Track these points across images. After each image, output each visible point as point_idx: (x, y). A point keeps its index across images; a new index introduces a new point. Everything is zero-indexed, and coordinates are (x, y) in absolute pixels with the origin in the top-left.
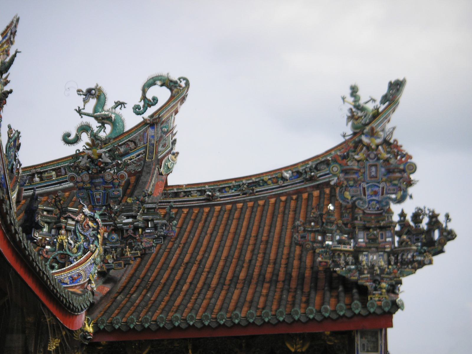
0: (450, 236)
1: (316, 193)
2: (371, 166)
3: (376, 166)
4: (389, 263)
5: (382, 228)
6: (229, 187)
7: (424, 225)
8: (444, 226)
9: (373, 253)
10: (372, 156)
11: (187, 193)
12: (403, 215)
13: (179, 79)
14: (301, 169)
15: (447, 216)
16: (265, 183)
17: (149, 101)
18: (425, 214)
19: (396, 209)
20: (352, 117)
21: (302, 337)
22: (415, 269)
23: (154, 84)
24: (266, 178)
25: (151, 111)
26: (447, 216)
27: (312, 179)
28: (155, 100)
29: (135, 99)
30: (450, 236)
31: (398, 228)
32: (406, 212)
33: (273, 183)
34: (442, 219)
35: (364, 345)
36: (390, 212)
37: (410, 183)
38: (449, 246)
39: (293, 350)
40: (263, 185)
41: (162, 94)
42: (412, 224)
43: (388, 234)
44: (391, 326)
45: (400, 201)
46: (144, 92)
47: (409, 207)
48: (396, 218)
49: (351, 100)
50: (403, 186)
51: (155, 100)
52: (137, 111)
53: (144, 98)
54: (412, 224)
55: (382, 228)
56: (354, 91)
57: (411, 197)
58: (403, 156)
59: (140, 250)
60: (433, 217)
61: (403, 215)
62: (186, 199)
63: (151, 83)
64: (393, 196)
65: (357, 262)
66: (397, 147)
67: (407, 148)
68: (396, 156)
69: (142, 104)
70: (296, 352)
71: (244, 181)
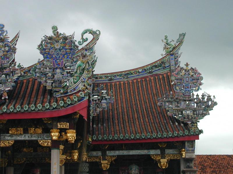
0: (216, 104)
1: (152, 78)
2: (187, 77)
3: (188, 77)
4: (194, 114)
5: (190, 100)
6: (118, 75)
7: (206, 100)
8: (213, 100)
9: (188, 110)
10: (187, 74)
11: (101, 78)
13: (96, 31)
14: (145, 68)
15: (214, 96)
16: (132, 74)
17: (84, 39)
18: (206, 96)
19: (195, 93)
21: (165, 142)
22: (203, 116)
23: (86, 32)
24: (132, 72)
25: (85, 43)
26: (214, 96)
27: (150, 73)
28: (87, 39)
30: (216, 104)
31: (196, 100)
32: (198, 94)
33: (135, 74)
34: (212, 97)
35: (188, 146)
37: (201, 84)
38: (215, 108)
39: (161, 146)
40: (131, 75)
41: (90, 37)
42: (201, 99)
43: (193, 103)
44: (198, 139)
45: (198, 90)
46: (82, 36)
47: (200, 93)
48: (195, 97)
49: (165, 41)
50: (198, 85)
51: (87, 39)
54: (201, 99)
55: (190, 100)
56: (166, 38)
57: (201, 89)
59: (102, 108)
60: (209, 96)
61: (197, 95)
62: (100, 79)
63: (85, 32)
64: (194, 89)
65: (182, 114)
66: (196, 70)
67: (199, 71)
68: (195, 74)
69: (81, 41)
70: (162, 147)
71: (123, 73)
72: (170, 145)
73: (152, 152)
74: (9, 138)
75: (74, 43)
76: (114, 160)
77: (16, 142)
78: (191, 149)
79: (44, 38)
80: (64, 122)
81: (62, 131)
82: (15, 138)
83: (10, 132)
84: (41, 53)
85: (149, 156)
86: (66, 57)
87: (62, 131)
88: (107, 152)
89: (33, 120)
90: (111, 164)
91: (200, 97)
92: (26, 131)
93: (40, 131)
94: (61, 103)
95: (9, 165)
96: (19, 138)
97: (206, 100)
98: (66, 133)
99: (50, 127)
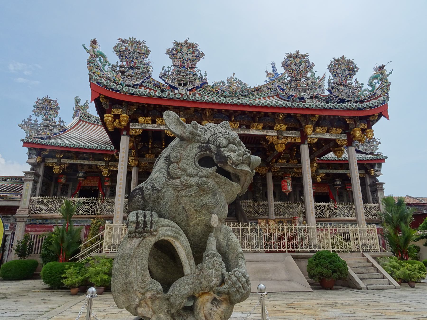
44: (384, 162)
75: (355, 66)
77: (320, 139)
78: (379, 169)
79: (333, 60)
80: (364, 123)
82: (319, 136)
84: (330, 72)
86: (349, 77)
95: (270, 170)
96: (322, 136)
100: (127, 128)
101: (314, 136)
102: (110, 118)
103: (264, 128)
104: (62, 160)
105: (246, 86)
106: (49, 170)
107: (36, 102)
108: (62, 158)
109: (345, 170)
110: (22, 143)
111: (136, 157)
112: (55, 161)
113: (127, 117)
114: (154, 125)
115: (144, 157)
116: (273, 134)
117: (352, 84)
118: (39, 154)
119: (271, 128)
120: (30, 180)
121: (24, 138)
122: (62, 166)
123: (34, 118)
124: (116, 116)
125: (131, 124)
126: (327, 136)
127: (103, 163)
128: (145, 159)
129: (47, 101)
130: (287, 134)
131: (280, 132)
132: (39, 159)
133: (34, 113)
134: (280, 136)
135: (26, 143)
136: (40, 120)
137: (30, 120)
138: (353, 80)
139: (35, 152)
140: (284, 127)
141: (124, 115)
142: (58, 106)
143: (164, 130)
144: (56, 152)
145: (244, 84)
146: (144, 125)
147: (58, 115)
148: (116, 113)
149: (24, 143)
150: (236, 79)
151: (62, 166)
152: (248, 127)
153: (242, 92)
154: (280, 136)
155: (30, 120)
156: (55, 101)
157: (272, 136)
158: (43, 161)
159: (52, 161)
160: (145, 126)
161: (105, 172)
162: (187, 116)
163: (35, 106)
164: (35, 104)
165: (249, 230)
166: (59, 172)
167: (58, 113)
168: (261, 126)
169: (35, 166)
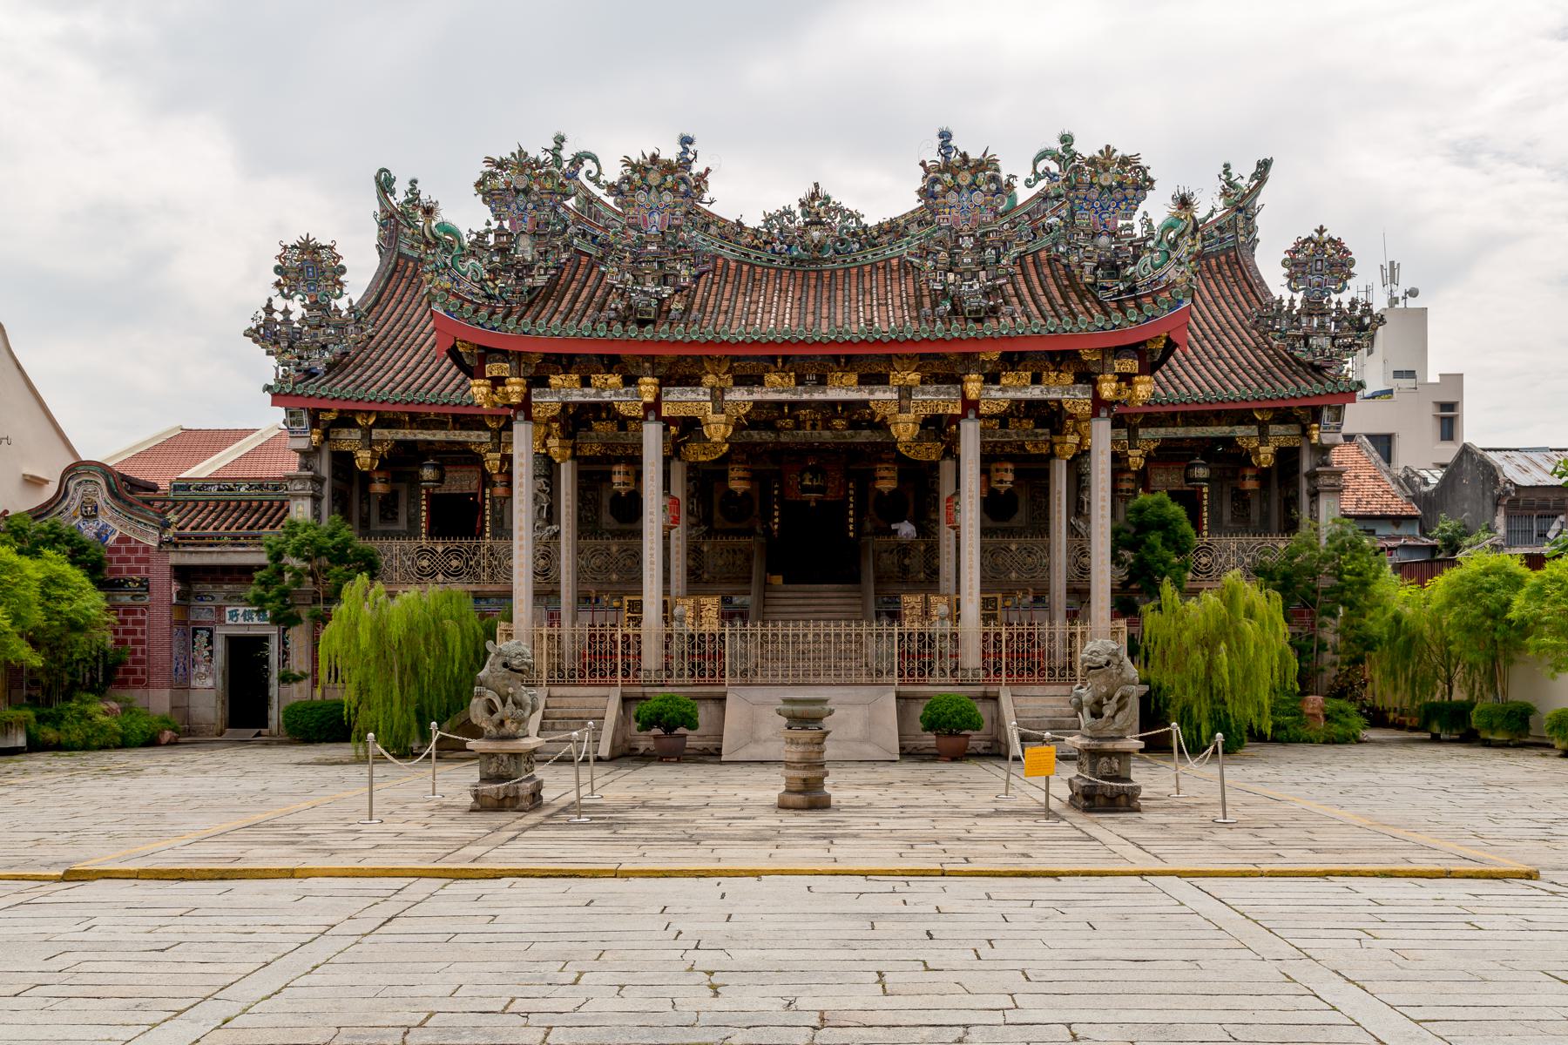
7: (1358, 313)
12: (1339, 303)
20: (1225, 193)
29: (1025, 173)
36: (1330, 301)
37: (1350, 275)
45: (1340, 291)
47: (1345, 298)
48: (1333, 306)
52: (1028, 184)
53: (1035, 172)
58: (1346, 251)
61: (1339, 303)
65: (1306, 344)
72: (1284, 416)
73: (1240, 431)
74: (999, 395)
76: (1157, 449)
81: (1126, 378)
82: (1011, 394)
83: (1004, 381)
85: (1229, 441)
87: (1126, 378)
88: (1141, 431)
89: (1051, 355)
90: (1148, 458)
91: (1346, 305)
92: (1036, 380)
93: (1068, 378)
94: (1117, 318)
96: (1020, 395)
97: (1358, 313)
98: (1130, 384)
99: (1094, 369)
100: (525, 406)
101: (999, 395)
102: (484, 390)
103: (865, 380)
104: (374, 431)
105: (858, 220)
106: (343, 461)
107: (279, 257)
108: (374, 426)
109: (1231, 424)
110: (268, 396)
111: (566, 437)
112: (356, 434)
113: (519, 384)
114: (587, 390)
115: (591, 429)
116: (888, 396)
117: (1131, 227)
118: (315, 423)
119: (882, 380)
120: (303, 496)
121: (272, 383)
122: (378, 448)
123: (279, 304)
124: (498, 382)
125: (534, 391)
126: (1035, 393)
127: (485, 436)
128: (593, 434)
129: (308, 249)
130: (924, 393)
131: (906, 391)
132: (315, 437)
133: (277, 291)
134: (904, 402)
135: (278, 395)
136: (297, 309)
137: (269, 309)
138: (1138, 215)
139: (305, 418)
140: (914, 377)
141: (513, 380)
142: (341, 262)
143: (611, 403)
144: (354, 412)
145: (851, 215)
146: (563, 391)
147: (345, 290)
148: (495, 374)
149: (274, 395)
150: (828, 198)
151: (378, 448)
152: (822, 381)
153: (843, 242)
154: (904, 402)
155: (269, 309)
156: (332, 248)
157: (885, 402)
158: (326, 436)
159: (349, 439)
160: (567, 395)
161: (492, 461)
162: (662, 370)
163: (278, 270)
164: (278, 263)
165: (810, 638)
166: (371, 466)
167: (341, 284)
168: (854, 378)
169: (307, 455)
